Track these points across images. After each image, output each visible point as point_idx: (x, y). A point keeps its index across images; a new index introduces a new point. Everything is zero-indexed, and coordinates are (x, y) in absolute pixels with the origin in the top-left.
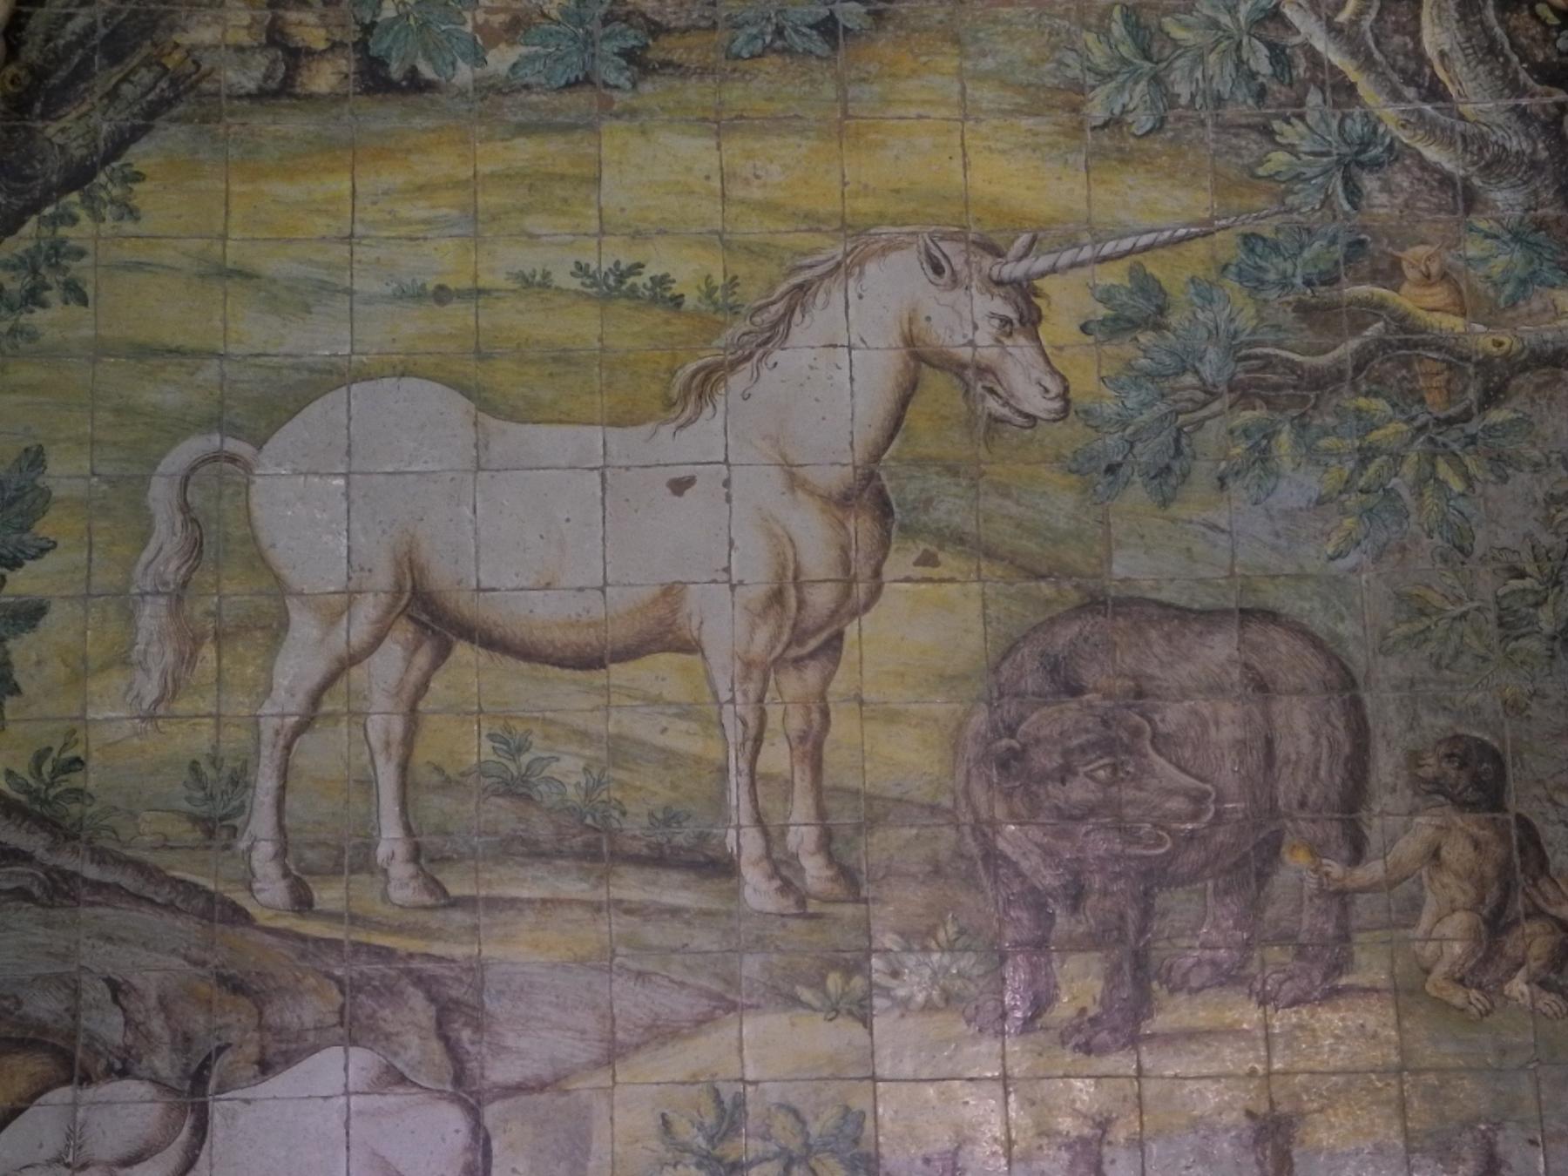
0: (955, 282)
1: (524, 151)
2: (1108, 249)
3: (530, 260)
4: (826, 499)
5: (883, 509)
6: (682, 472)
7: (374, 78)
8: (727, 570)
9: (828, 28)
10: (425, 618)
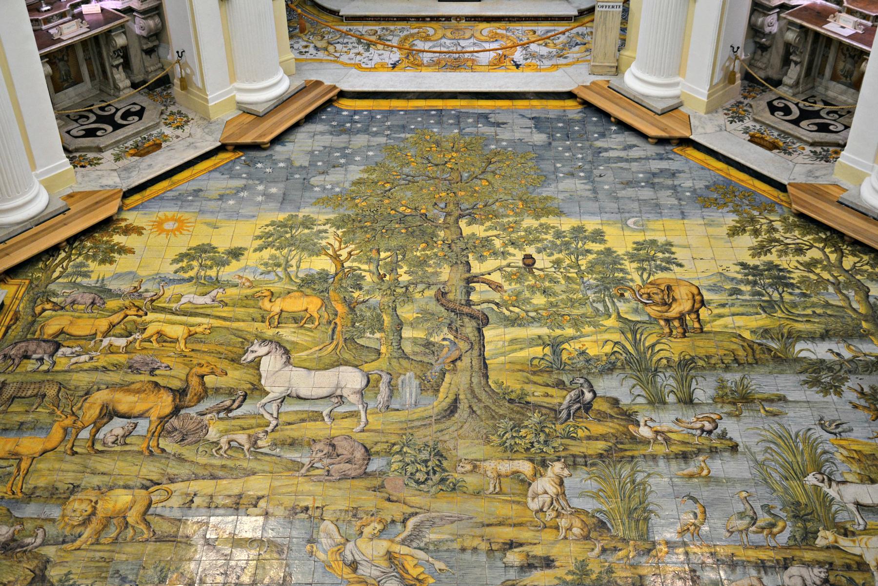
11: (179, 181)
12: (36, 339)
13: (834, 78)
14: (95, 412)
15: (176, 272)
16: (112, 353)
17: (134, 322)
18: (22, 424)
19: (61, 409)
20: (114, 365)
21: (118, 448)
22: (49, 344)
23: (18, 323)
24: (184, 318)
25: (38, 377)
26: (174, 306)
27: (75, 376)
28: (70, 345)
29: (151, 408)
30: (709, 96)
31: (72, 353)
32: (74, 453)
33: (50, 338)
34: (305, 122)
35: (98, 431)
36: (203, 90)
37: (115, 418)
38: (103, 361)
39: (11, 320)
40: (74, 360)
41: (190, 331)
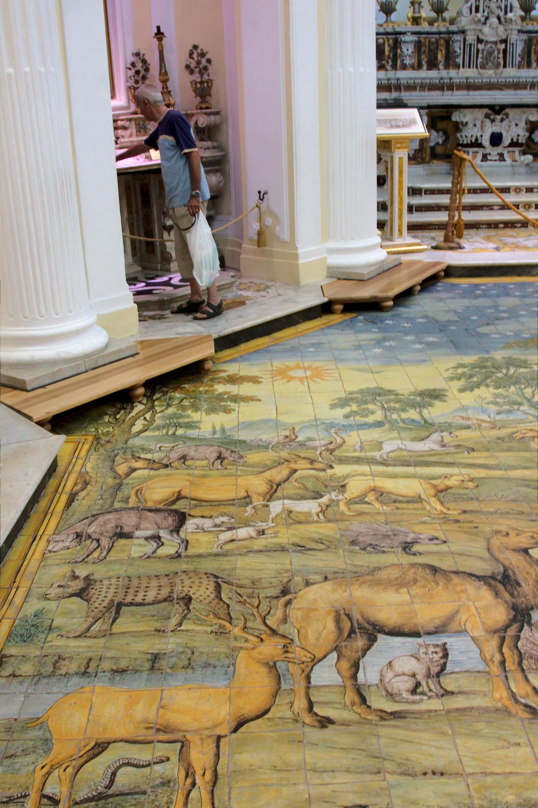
11: (285, 337)
12: (133, 509)
14: (320, 631)
15: (347, 416)
16: (299, 522)
17: (317, 478)
18: (156, 657)
19: (241, 624)
20: (320, 541)
21: (435, 704)
22: (162, 515)
23: (89, 487)
24: (411, 470)
25: (161, 567)
26: (377, 454)
27: (241, 562)
28: (207, 513)
29: (457, 612)
31: (216, 526)
32: (325, 722)
33: (161, 506)
34: (421, 291)
35: (356, 666)
36: (292, 243)
37: (380, 636)
38: (285, 536)
39: (76, 484)
40: (225, 536)
41: (434, 486)
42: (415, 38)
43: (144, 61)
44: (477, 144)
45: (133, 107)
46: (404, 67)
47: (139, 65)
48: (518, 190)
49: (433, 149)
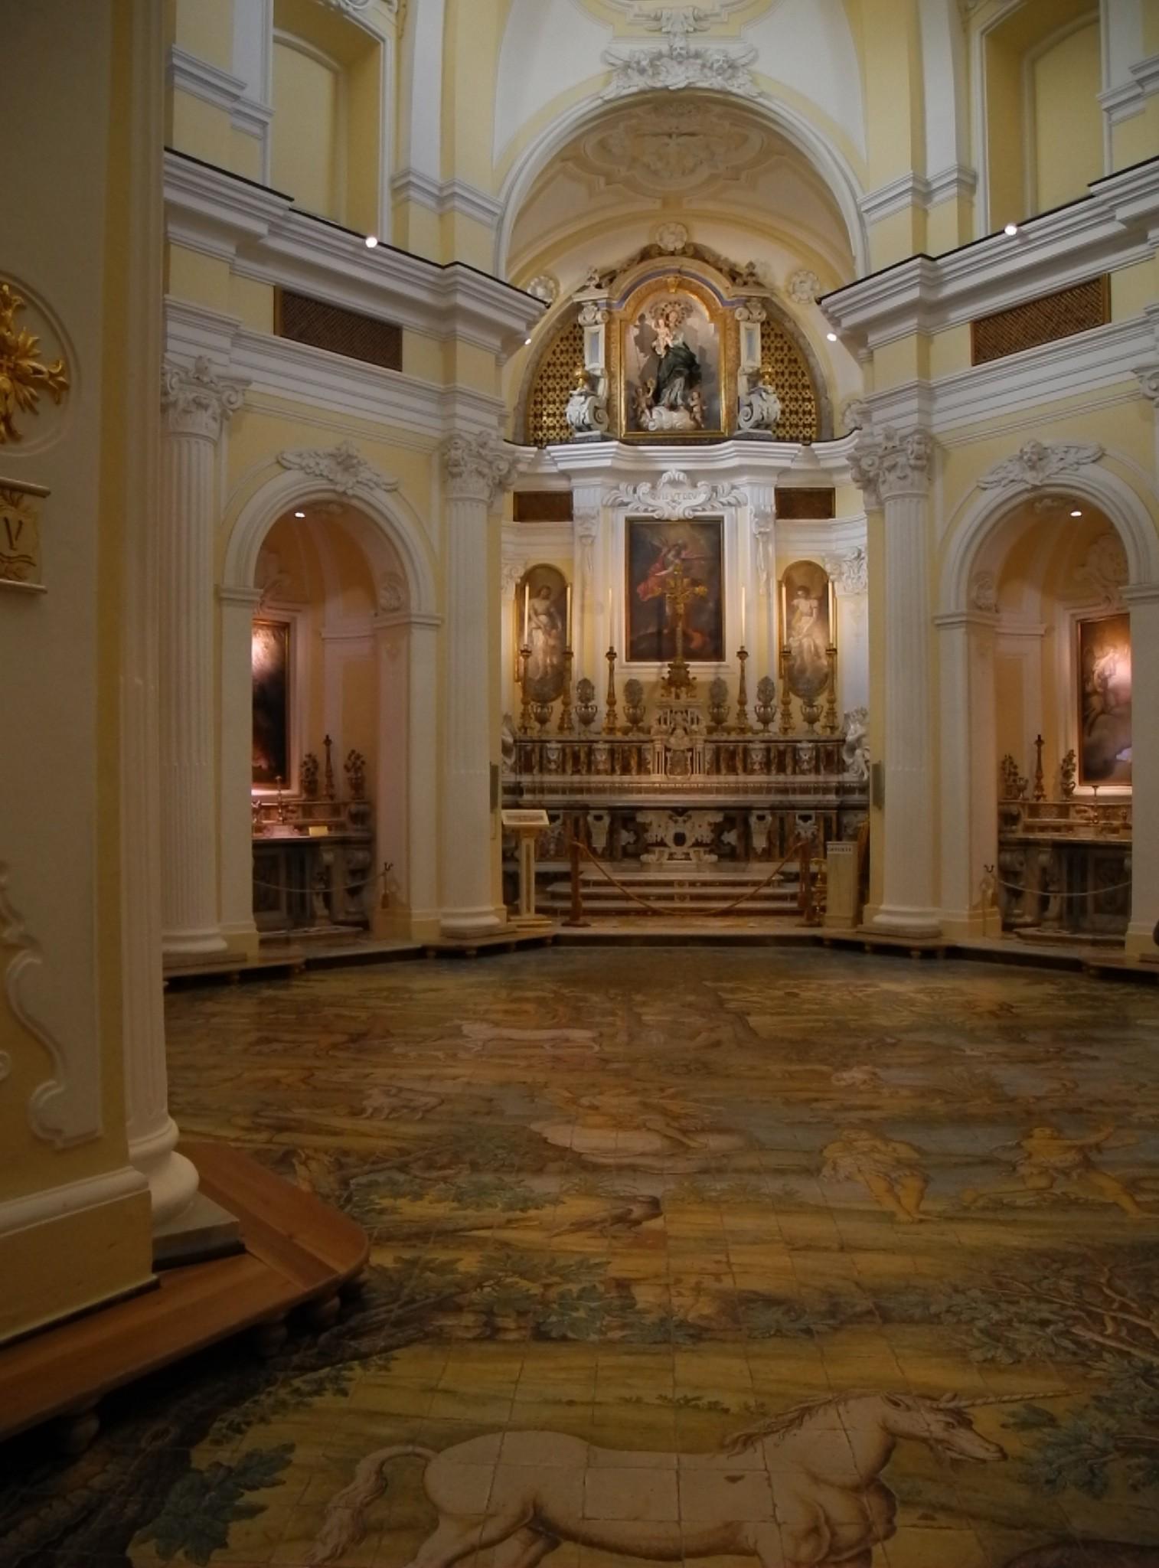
0: (908, 1408)
1: (627, 1360)
2: (1006, 1398)
3: (625, 1393)
4: (843, 1488)
5: (886, 1493)
6: (737, 1474)
7: (541, 1335)
8: (774, 1516)
9: (808, 1332)
10: (541, 1529)
13: (1099, 909)
30: (971, 917)
36: (408, 906)
42: (607, 746)
43: (314, 761)
44: (662, 844)
45: (304, 796)
46: (598, 772)
47: (310, 765)
48: (681, 884)
49: (624, 848)
